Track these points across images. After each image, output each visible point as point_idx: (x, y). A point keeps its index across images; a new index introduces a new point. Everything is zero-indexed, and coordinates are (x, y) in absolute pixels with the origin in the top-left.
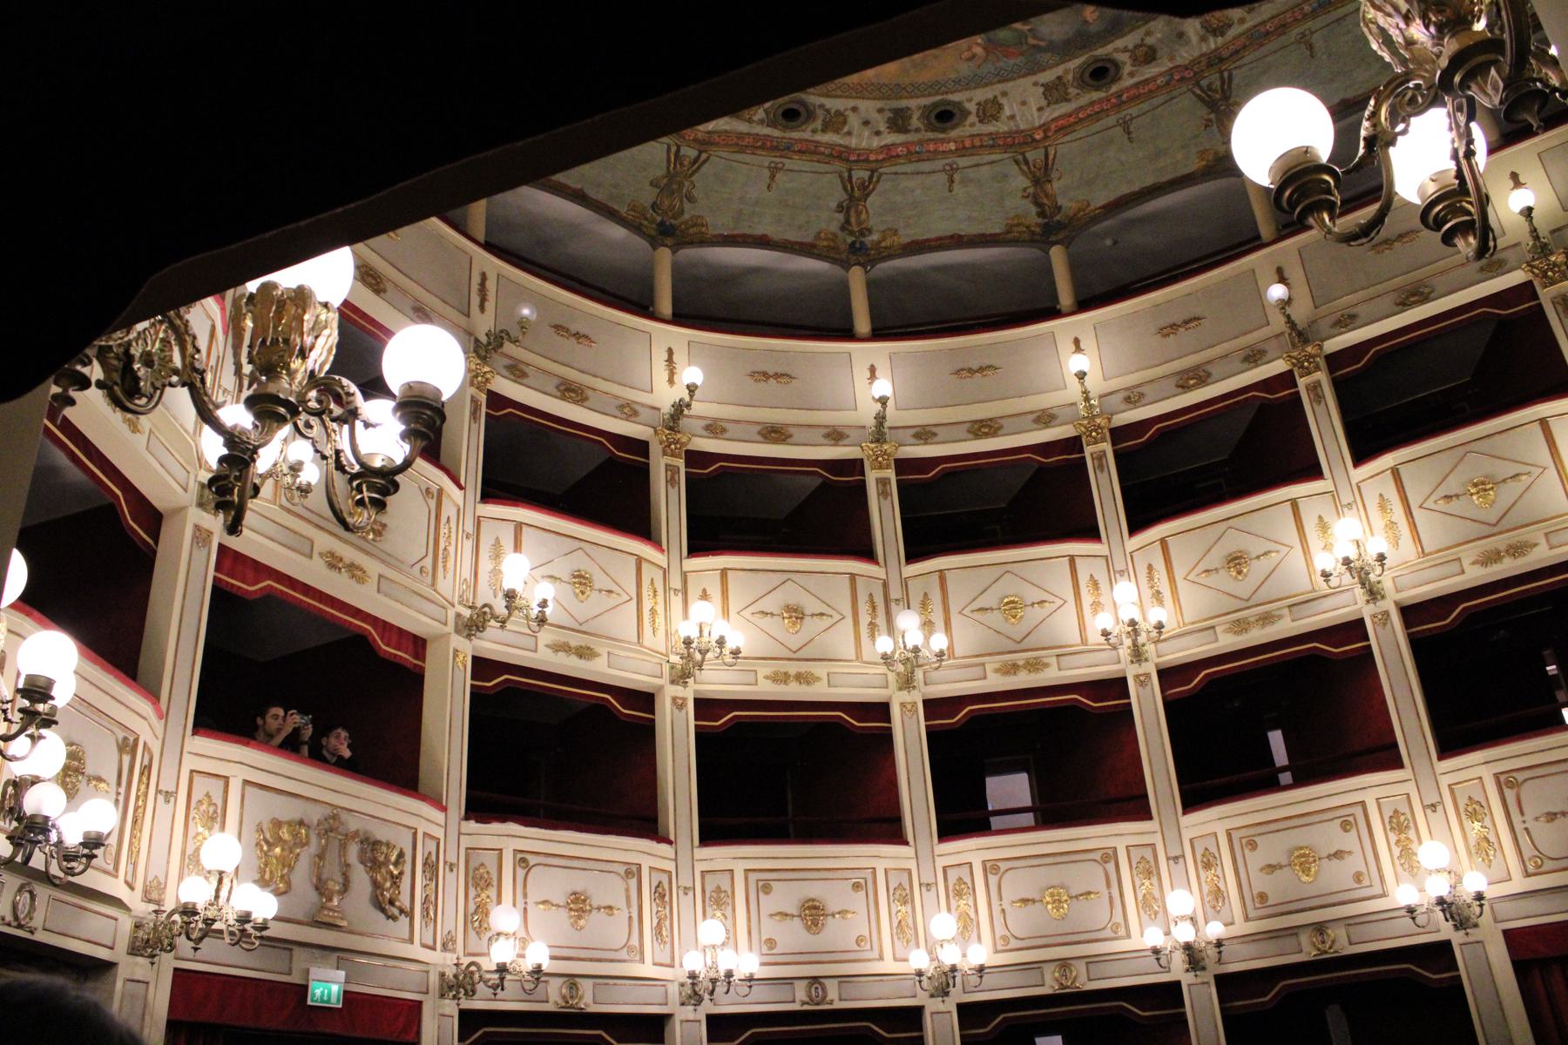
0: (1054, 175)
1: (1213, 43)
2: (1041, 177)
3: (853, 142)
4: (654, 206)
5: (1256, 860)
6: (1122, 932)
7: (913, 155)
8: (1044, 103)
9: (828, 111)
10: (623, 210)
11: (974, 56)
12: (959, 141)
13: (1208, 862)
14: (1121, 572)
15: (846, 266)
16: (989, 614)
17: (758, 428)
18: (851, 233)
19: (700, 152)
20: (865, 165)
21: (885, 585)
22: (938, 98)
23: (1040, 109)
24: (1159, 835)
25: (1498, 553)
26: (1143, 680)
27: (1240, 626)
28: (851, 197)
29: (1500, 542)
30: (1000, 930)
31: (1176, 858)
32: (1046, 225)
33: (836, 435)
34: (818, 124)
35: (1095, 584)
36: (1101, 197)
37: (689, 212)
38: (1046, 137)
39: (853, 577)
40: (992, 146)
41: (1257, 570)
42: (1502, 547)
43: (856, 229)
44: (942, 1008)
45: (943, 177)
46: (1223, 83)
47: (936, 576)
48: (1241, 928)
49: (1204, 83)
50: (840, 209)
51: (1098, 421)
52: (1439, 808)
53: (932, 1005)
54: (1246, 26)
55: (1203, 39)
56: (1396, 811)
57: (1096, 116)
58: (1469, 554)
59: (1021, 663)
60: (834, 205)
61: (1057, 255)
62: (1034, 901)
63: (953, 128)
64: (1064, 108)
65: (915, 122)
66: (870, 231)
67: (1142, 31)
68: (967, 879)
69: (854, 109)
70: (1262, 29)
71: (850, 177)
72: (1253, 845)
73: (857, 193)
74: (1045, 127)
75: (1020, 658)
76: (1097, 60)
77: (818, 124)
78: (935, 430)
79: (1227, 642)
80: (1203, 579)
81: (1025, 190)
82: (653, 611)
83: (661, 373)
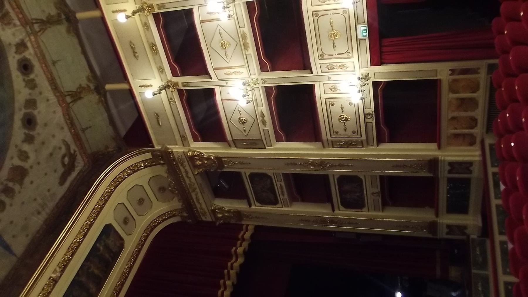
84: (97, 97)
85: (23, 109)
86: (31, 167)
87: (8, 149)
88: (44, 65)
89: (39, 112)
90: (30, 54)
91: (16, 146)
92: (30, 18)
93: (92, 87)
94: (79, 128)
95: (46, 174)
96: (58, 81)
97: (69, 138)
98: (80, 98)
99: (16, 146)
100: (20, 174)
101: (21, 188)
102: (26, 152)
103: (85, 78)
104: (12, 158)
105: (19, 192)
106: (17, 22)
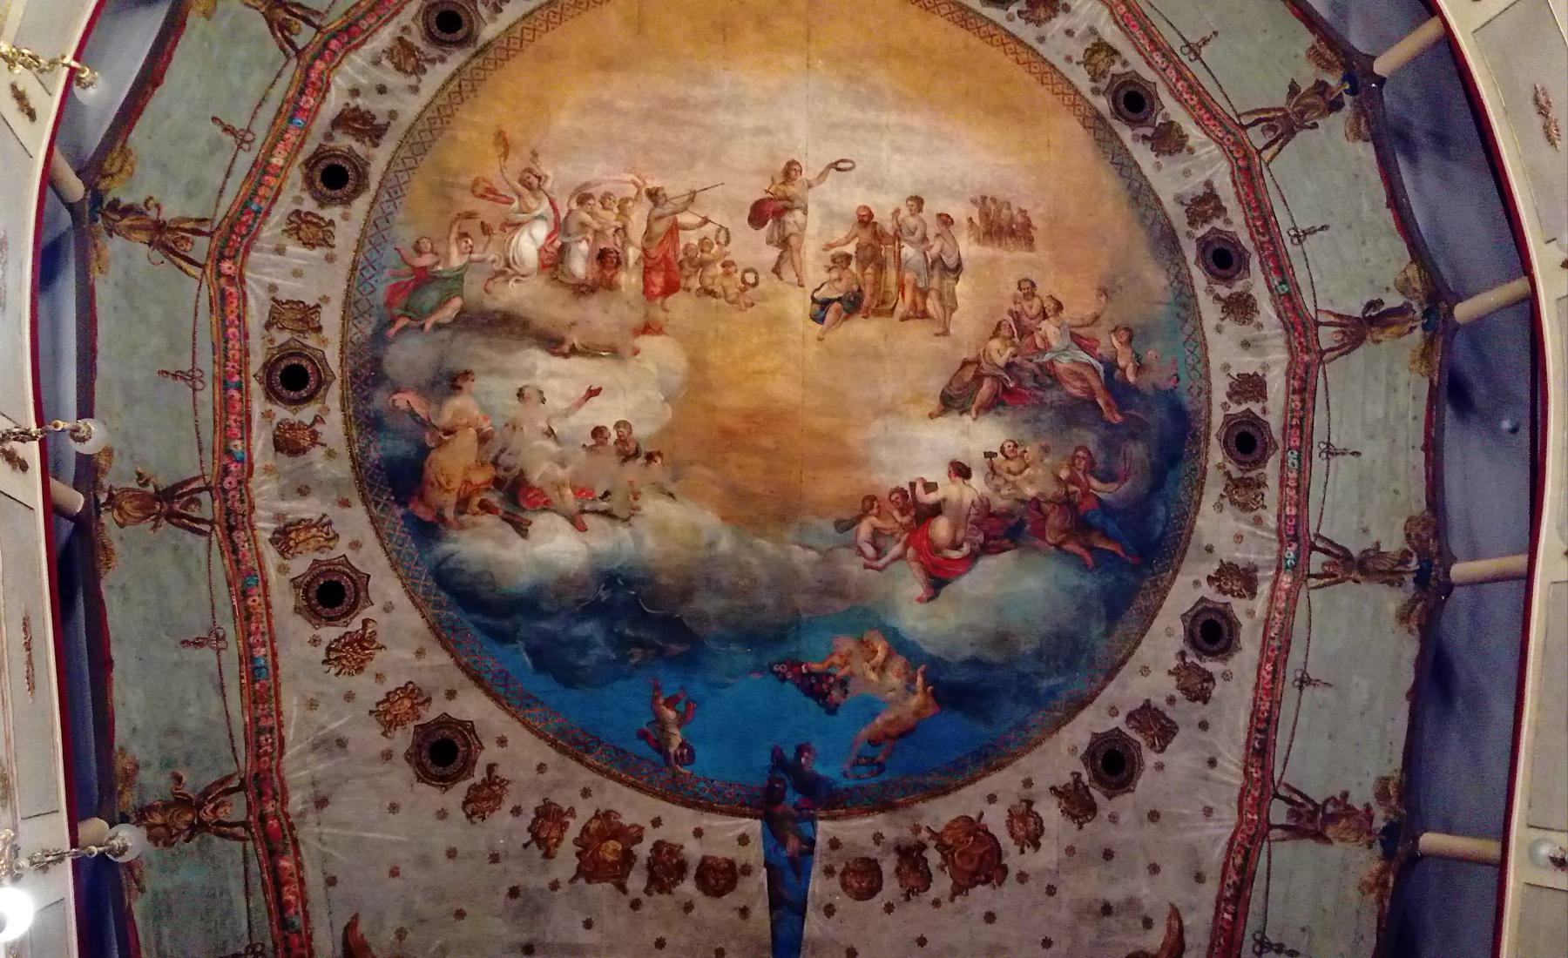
0: (157, 255)
1: (265, 527)
2: (165, 238)
3: (359, 58)
7: (293, 110)
8: (283, 296)
9: (432, 61)
11: (419, 251)
22: (374, 186)
23: (273, 288)
32: (101, 201)
34: (416, 39)
38: (220, 274)
40: (245, 207)
45: (240, 123)
49: (205, 497)
55: (279, 517)
57: (221, 348)
63: (309, 181)
64: (256, 315)
65: (343, 141)
67: (341, 448)
69: (415, 90)
73: (281, 14)
76: (322, 383)
77: (416, 39)
81: (158, 206)
84: (1377, 866)
85: (1121, 718)
86: (1022, 877)
87: (999, 767)
88: (1269, 667)
89: (1160, 767)
90: (1250, 613)
91: (1028, 783)
92: (1312, 530)
93: (1379, 823)
94: (1253, 923)
95: (1047, 943)
96: (1281, 739)
97: (1199, 925)
98: (1320, 837)
99: (1028, 783)
100: (977, 860)
101: (952, 900)
102: (1040, 829)
103: (1370, 783)
104: (992, 799)
106: (1271, 520)
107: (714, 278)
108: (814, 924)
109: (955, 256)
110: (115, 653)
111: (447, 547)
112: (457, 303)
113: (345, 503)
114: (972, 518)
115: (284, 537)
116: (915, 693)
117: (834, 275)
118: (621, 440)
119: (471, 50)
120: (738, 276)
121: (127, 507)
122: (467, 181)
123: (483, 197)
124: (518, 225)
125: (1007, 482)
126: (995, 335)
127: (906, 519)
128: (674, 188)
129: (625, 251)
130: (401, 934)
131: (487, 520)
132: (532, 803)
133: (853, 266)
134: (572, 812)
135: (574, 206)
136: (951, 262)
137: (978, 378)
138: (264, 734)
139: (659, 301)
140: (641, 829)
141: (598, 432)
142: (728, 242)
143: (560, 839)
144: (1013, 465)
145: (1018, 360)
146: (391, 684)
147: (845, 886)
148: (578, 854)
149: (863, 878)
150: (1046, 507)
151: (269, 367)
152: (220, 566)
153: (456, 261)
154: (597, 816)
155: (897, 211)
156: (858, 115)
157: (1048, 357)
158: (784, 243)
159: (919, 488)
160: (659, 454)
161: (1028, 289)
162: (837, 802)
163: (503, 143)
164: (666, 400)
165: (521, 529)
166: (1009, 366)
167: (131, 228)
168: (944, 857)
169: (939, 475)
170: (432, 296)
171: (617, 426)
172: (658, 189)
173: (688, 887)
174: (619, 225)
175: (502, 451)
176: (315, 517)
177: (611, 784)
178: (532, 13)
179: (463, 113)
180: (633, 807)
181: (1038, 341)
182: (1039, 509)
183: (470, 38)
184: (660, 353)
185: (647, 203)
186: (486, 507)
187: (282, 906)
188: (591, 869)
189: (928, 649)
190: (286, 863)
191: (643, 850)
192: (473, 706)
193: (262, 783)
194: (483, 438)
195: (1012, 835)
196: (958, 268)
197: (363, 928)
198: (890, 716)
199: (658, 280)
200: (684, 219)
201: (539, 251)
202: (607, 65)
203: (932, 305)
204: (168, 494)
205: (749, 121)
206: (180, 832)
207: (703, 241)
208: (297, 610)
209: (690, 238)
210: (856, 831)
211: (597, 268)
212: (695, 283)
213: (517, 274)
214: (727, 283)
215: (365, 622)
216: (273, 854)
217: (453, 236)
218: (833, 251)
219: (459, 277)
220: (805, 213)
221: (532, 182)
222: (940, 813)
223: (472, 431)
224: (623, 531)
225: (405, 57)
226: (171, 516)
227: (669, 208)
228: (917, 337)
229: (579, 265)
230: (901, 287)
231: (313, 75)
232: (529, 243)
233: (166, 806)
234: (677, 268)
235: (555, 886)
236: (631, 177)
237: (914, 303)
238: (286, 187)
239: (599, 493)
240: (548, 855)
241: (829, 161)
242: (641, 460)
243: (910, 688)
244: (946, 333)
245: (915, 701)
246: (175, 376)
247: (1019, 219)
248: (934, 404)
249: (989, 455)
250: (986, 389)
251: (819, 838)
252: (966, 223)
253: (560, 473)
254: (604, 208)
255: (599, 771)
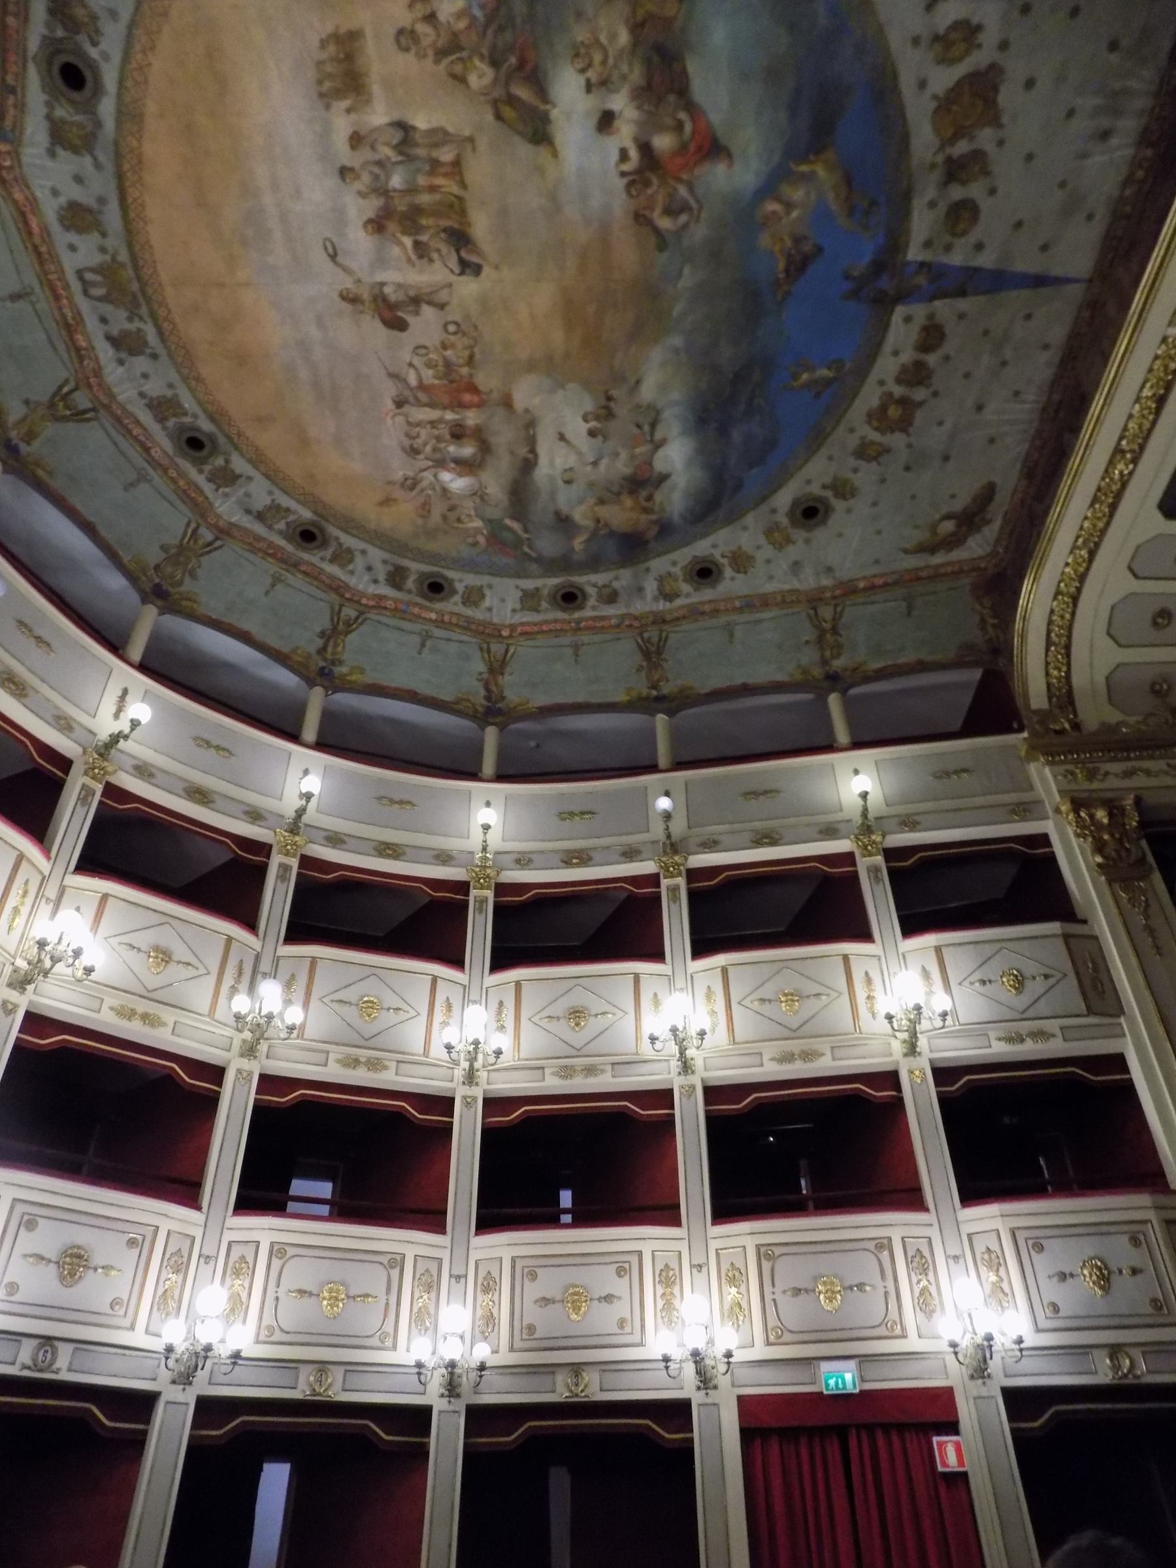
0: (508, 670)
1: (662, 605)
2: (497, 668)
3: (352, 581)
4: (157, 568)
5: (533, 1291)
6: (389, 1343)
7: (400, 612)
8: (518, 606)
9: (340, 545)
10: (126, 560)
12: (440, 613)
13: (488, 1286)
14: (475, 1002)
15: (311, 683)
16: (346, 1008)
17: (186, 785)
18: (325, 659)
19: (217, 539)
20: (356, 606)
21: (258, 958)
23: (514, 611)
24: (448, 1251)
25: (793, 1055)
26: (469, 1102)
27: (567, 1072)
28: (334, 629)
29: (795, 1046)
30: (268, 1320)
31: (458, 1277)
33: (255, 815)
34: (328, 553)
35: (449, 1006)
36: (541, 699)
37: (188, 586)
38: (511, 636)
39: (230, 940)
41: (592, 1026)
42: (797, 1052)
43: (329, 656)
44: (181, 1398)
45: (417, 639)
46: (660, 640)
47: (307, 962)
48: (505, 1358)
49: (646, 635)
50: (322, 634)
51: (488, 871)
52: (704, 1269)
53: (170, 1393)
54: (689, 601)
55: (655, 599)
56: (667, 1266)
57: (558, 633)
58: (770, 1051)
59: (362, 1060)
60: (318, 629)
61: (491, 736)
62: (311, 1294)
63: (442, 600)
65: (410, 583)
66: (341, 663)
68: (250, 1260)
69: (364, 552)
70: (701, 608)
71: (340, 610)
72: (533, 1276)
73: (341, 627)
74: (513, 627)
75: (363, 1054)
76: (572, 585)
77: (328, 553)
78: (346, 839)
79: (552, 1084)
80: (545, 1023)
82: (16, 911)
83: (108, 706)
87: (895, 76)
91: (916, 41)
99: (916, 41)
104: (922, 84)
105: (1001, 143)
107: (458, 357)
108: (986, 260)
109: (391, 130)
110: (739, 681)
111: (676, 517)
112: (508, 522)
113: (648, 570)
114: (653, 109)
115: (669, 597)
116: (813, 173)
117: (435, 256)
118: (597, 418)
119: (324, 524)
120: (452, 338)
121: (656, 677)
122: (420, 521)
123: (429, 511)
124: (445, 490)
125: (615, 66)
126: (462, 80)
127: (655, 181)
128: (389, 390)
129: (447, 422)
130: (917, 527)
131: (658, 497)
132: (852, 462)
133: (424, 238)
134: (863, 438)
135: (422, 456)
136: (397, 136)
137: (512, 100)
138: (785, 600)
139: (484, 397)
140: (884, 393)
141: (592, 433)
142: (425, 347)
143: (880, 444)
144: (597, 58)
145: (485, 51)
146: (762, 540)
147: (964, 233)
148: (893, 431)
149: (961, 215)
150: (641, 14)
151: (564, 610)
152: (685, 626)
153: (478, 523)
154: (869, 423)
155: (360, 194)
156: (278, 235)
157: (477, 12)
158: (416, 301)
159: (626, 167)
160: (606, 392)
161: (405, 38)
162: (895, 242)
163: (387, 502)
164: (562, 387)
165: (664, 478)
166: (495, 63)
167: (496, 684)
168: (963, 136)
169: (612, 145)
170: (506, 535)
171: (586, 420)
172: (394, 402)
173: (932, 359)
174: (428, 426)
175: (608, 490)
176: (655, 585)
177: (848, 416)
178: (281, 489)
179: (372, 526)
180: (869, 397)
181: (462, 25)
182: (642, 25)
183: (313, 523)
184: (525, 394)
185: (406, 409)
186: (650, 498)
187: (886, 585)
188: (904, 425)
189: (776, 158)
190: (862, 585)
191: (898, 391)
192: (784, 499)
193: (814, 600)
194: (601, 502)
195: (960, 59)
196: (402, 126)
197: (908, 546)
198: (831, 196)
199: (467, 397)
200: (413, 380)
201: (460, 475)
202: (304, 442)
203: (446, 155)
204: (647, 655)
205: (315, 333)
206: (836, 641)
207: (429, 365)
208: (713, 587)
209: (428, 376)
210: (922, 222)
211: (465, 440)
212: (465, 371)
213: (481, 488)
214: (460, 346)
215: (723, 556)
216: (855, 591)
217: (461, 526)
218: (414, 257)
219: (489, 522)
220: (383, 284)
221: (411, 484)
222: (924, 139)
223: (597, 508)
224: (667, 414)
225: (343, 557)
226: (659, 652)
227: (407, 393)
228: (481, 170)
229: (467, 450)
230: (433, 189)
231: (372, 603)
232: (457, 483)
233: (822, 649)
234: (454, 385)
235: (910, 446)
236: (389, 421)
237: (446, 175)
238: (449, 609)
239: (636, 431)
240: (888, 451)
241: (330, 264)
242: (612, 404)
243: (810, 177)
244: (471, 140)
245: (821, 172)
246: (577, 656)
247: (332, 49)
248: (543, 152)
249: (589, 87)
250: (523, 92)
251: (920, 258)
252: (353, 116)
253: (624, 455)
254: (418, 436)
255: (838, 422)
